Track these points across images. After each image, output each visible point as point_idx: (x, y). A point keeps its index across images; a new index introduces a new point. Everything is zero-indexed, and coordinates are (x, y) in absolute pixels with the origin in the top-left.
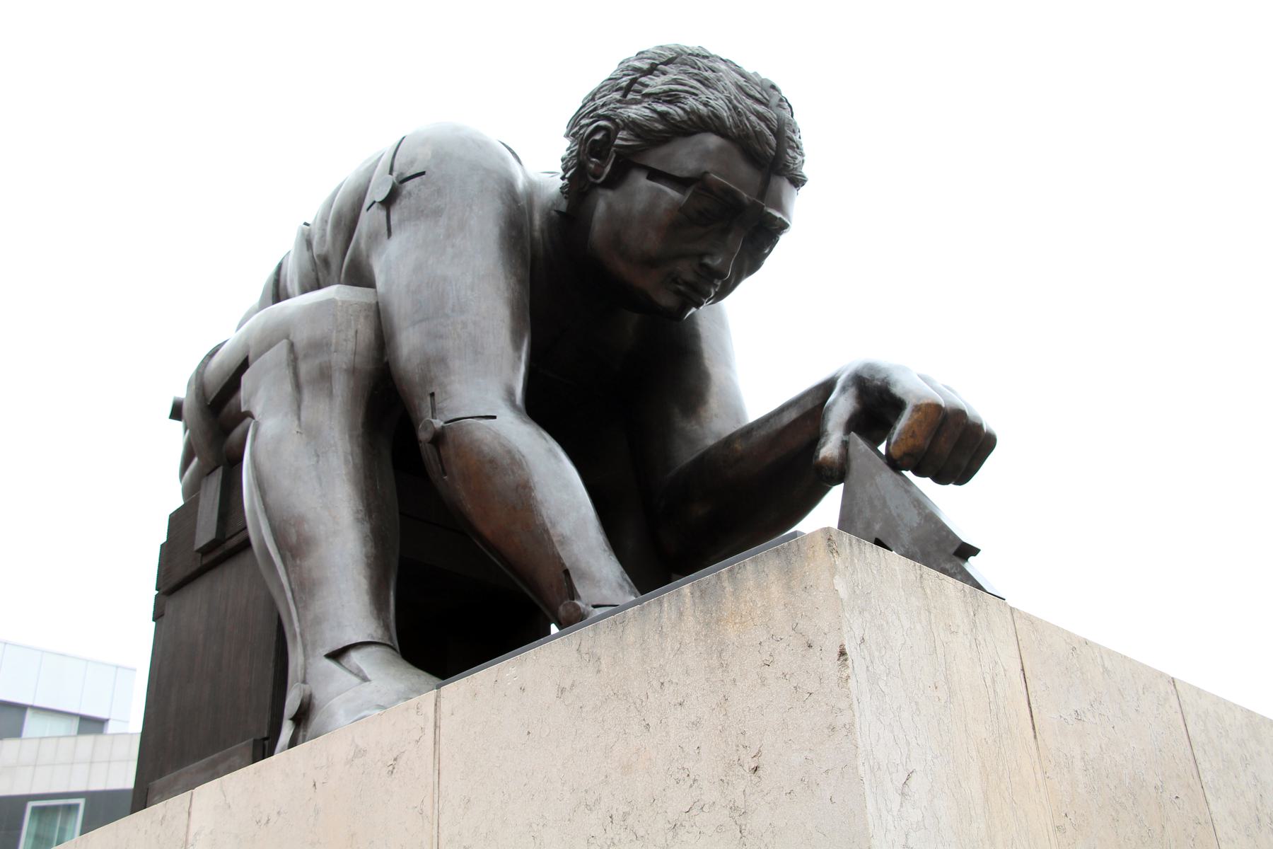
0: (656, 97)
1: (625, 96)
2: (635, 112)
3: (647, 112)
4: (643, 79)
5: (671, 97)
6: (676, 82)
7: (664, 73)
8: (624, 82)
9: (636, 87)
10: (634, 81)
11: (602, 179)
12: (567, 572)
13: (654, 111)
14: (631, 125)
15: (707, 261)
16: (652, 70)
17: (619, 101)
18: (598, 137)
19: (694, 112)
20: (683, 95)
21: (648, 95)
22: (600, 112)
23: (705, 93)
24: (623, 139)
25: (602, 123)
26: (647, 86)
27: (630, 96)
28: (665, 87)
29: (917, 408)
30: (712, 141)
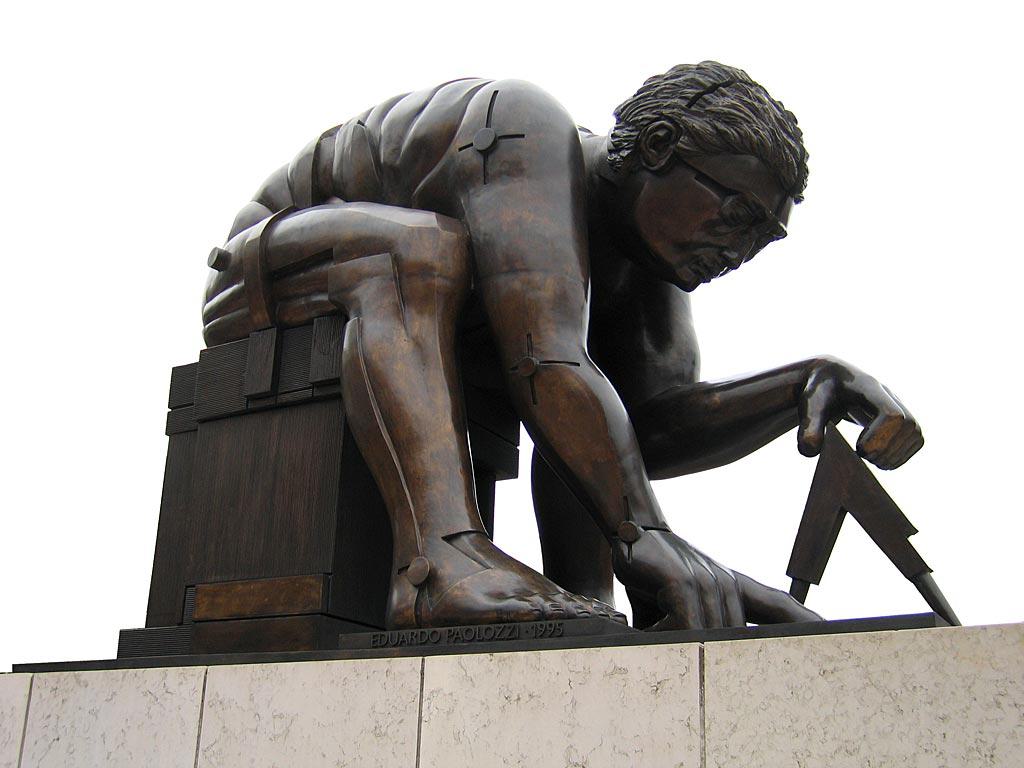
0: (718, 115)
1: (689, 106)
2: (696, 123)
3: (709, 128)
4: (706, 96)
5: (729, 119)
6: (733, 106)
7: (724, 95)
8: (691, 92)
9: (700, 101)
10: (699, 96)
11: (656, 168)
12: (625, 498)
13: (715, 128)
14: (693, 134)
16: (714, 88)
17: (683, 109)
18: (661, 133)
19: (744, 137)
20: (740, 120)
22: (665, 112)
23: (758, 124)
24: (683, 142)
26: (710, 103)
27: (693, 108)
28: (726, 109)
29: (889, 418)
30: (753, 161)
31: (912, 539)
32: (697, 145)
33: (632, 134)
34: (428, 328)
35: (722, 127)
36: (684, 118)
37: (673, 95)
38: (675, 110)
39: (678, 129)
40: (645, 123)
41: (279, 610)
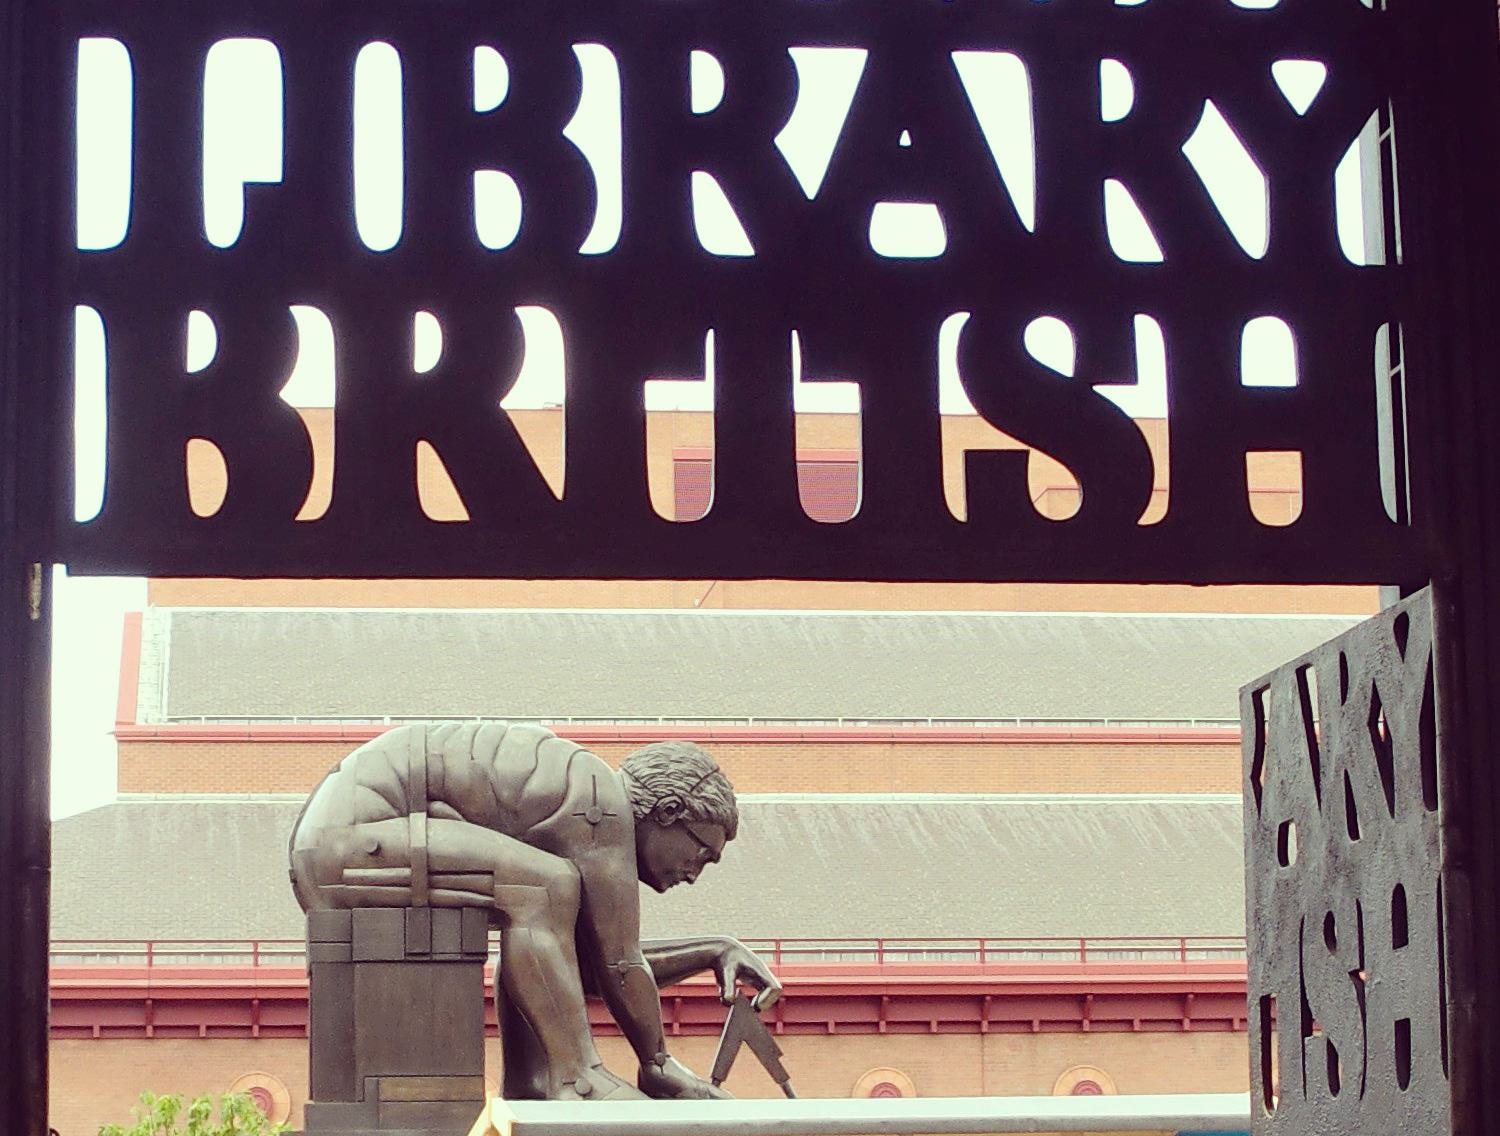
1: (692, 790)
2: (697, 804)
5: (713, 803)
6: (716, 794)
14: (693, 812)
15: (689, 875)
21: (703, 797)
22: (677, 791)
25: (679, 801)
27: (695, 793)
28: (713, 796)
31: (781, 1059)
32: (693, 816)
33: (651, 798)
34: (568, 937)
35: (710, 808)
36: (687, 798)
37: (681, 779)
38: (682, 791)
39: (682, 806)
40: (663, 795)
41: (454, 1097)
